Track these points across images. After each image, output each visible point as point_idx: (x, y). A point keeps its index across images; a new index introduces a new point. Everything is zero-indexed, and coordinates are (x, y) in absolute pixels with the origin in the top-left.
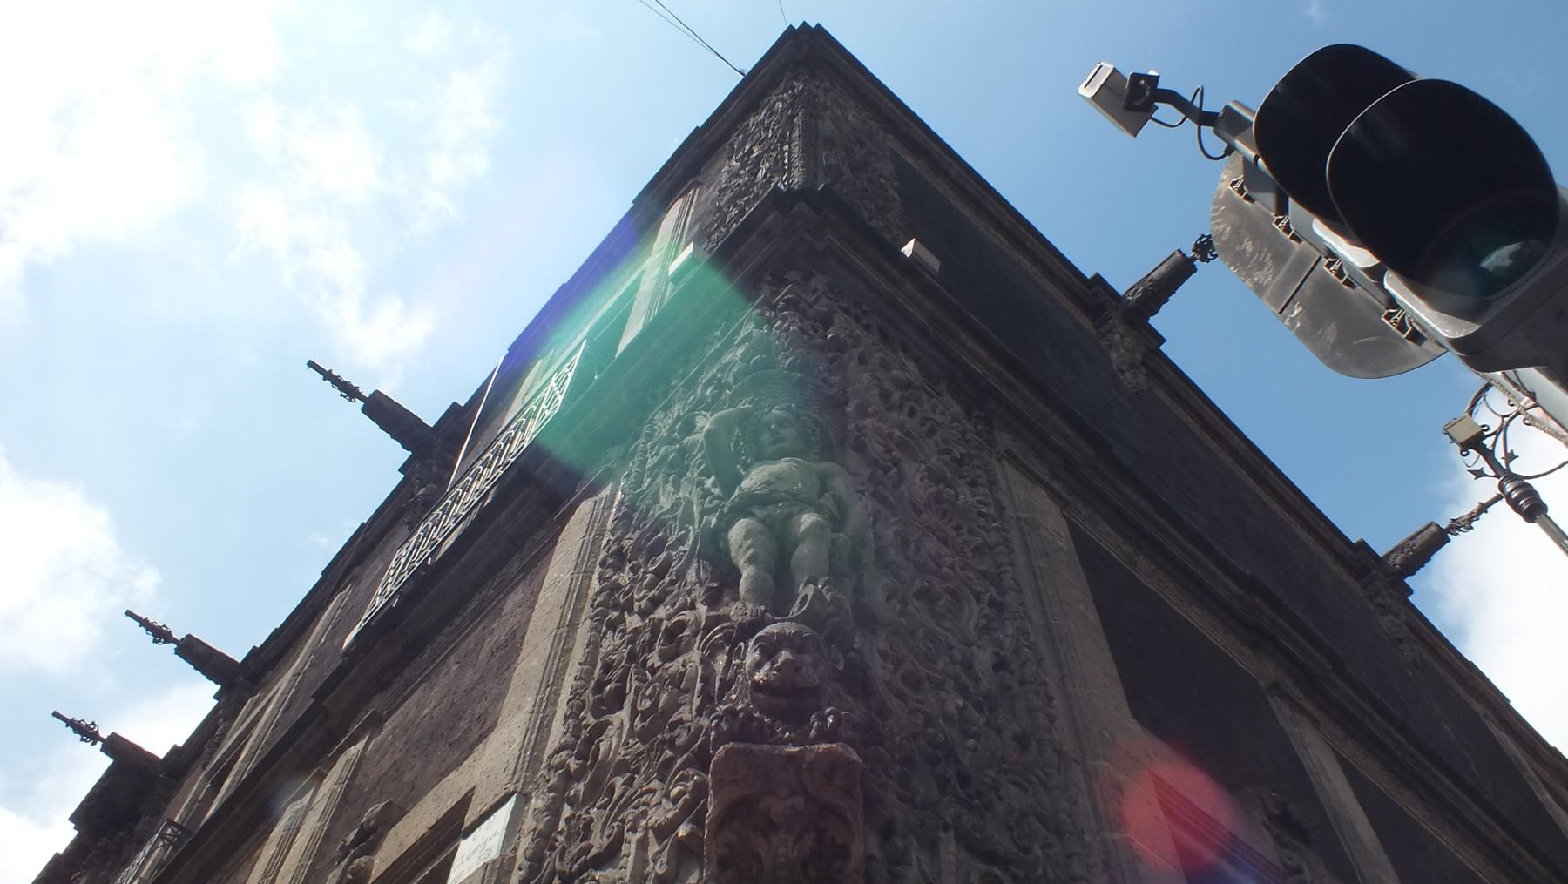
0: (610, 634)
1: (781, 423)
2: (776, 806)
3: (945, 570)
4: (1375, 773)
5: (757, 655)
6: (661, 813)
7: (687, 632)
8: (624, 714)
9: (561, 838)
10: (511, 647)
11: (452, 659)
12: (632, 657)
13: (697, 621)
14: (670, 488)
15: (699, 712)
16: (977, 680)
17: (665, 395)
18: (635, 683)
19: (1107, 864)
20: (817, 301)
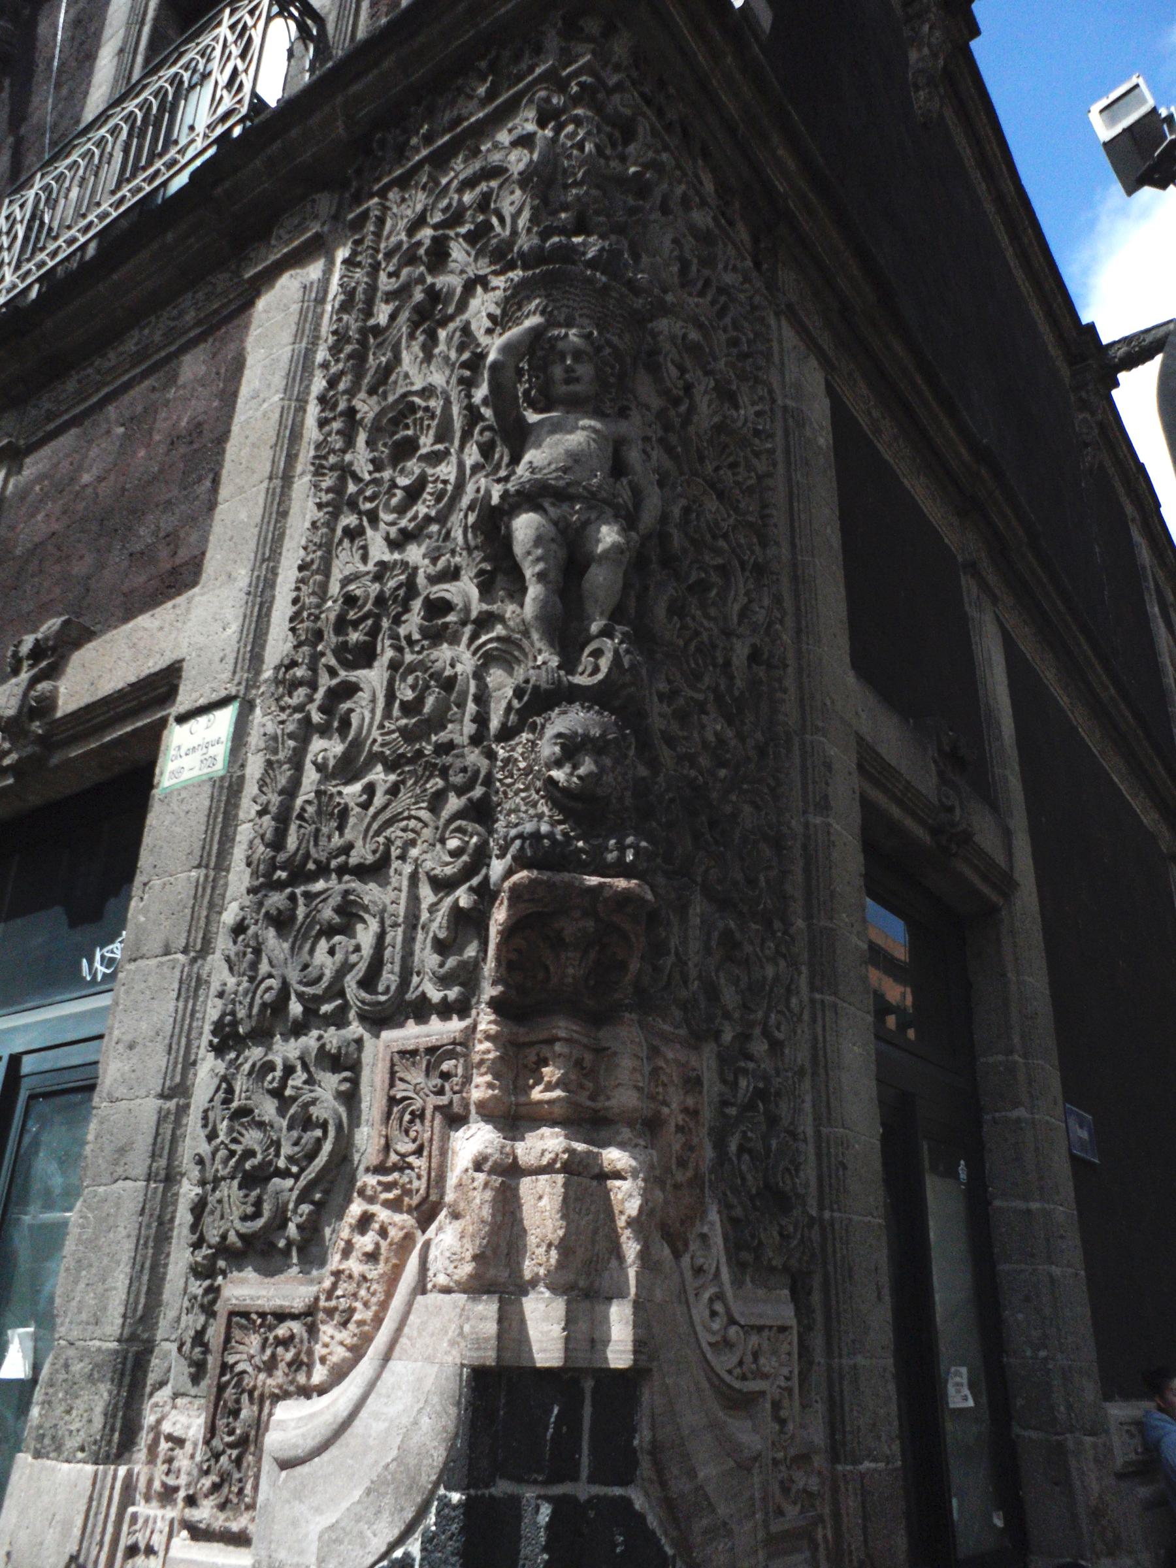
0: (346, 543)
1: (578, 355)
2: (570, 927)
3: (721, 543)
5: (557, 749)
6: (439, 862)
7: (451, 618)
8: (373, 678)
9: (311, 809)
11: (111, 410)
12: (380, 600)
13: (467, 609)
14: (416, 347)
15: (476, 740)
16: (732, 678)
18: (389, 653)
19: (805, 847)
20: (619, 87)
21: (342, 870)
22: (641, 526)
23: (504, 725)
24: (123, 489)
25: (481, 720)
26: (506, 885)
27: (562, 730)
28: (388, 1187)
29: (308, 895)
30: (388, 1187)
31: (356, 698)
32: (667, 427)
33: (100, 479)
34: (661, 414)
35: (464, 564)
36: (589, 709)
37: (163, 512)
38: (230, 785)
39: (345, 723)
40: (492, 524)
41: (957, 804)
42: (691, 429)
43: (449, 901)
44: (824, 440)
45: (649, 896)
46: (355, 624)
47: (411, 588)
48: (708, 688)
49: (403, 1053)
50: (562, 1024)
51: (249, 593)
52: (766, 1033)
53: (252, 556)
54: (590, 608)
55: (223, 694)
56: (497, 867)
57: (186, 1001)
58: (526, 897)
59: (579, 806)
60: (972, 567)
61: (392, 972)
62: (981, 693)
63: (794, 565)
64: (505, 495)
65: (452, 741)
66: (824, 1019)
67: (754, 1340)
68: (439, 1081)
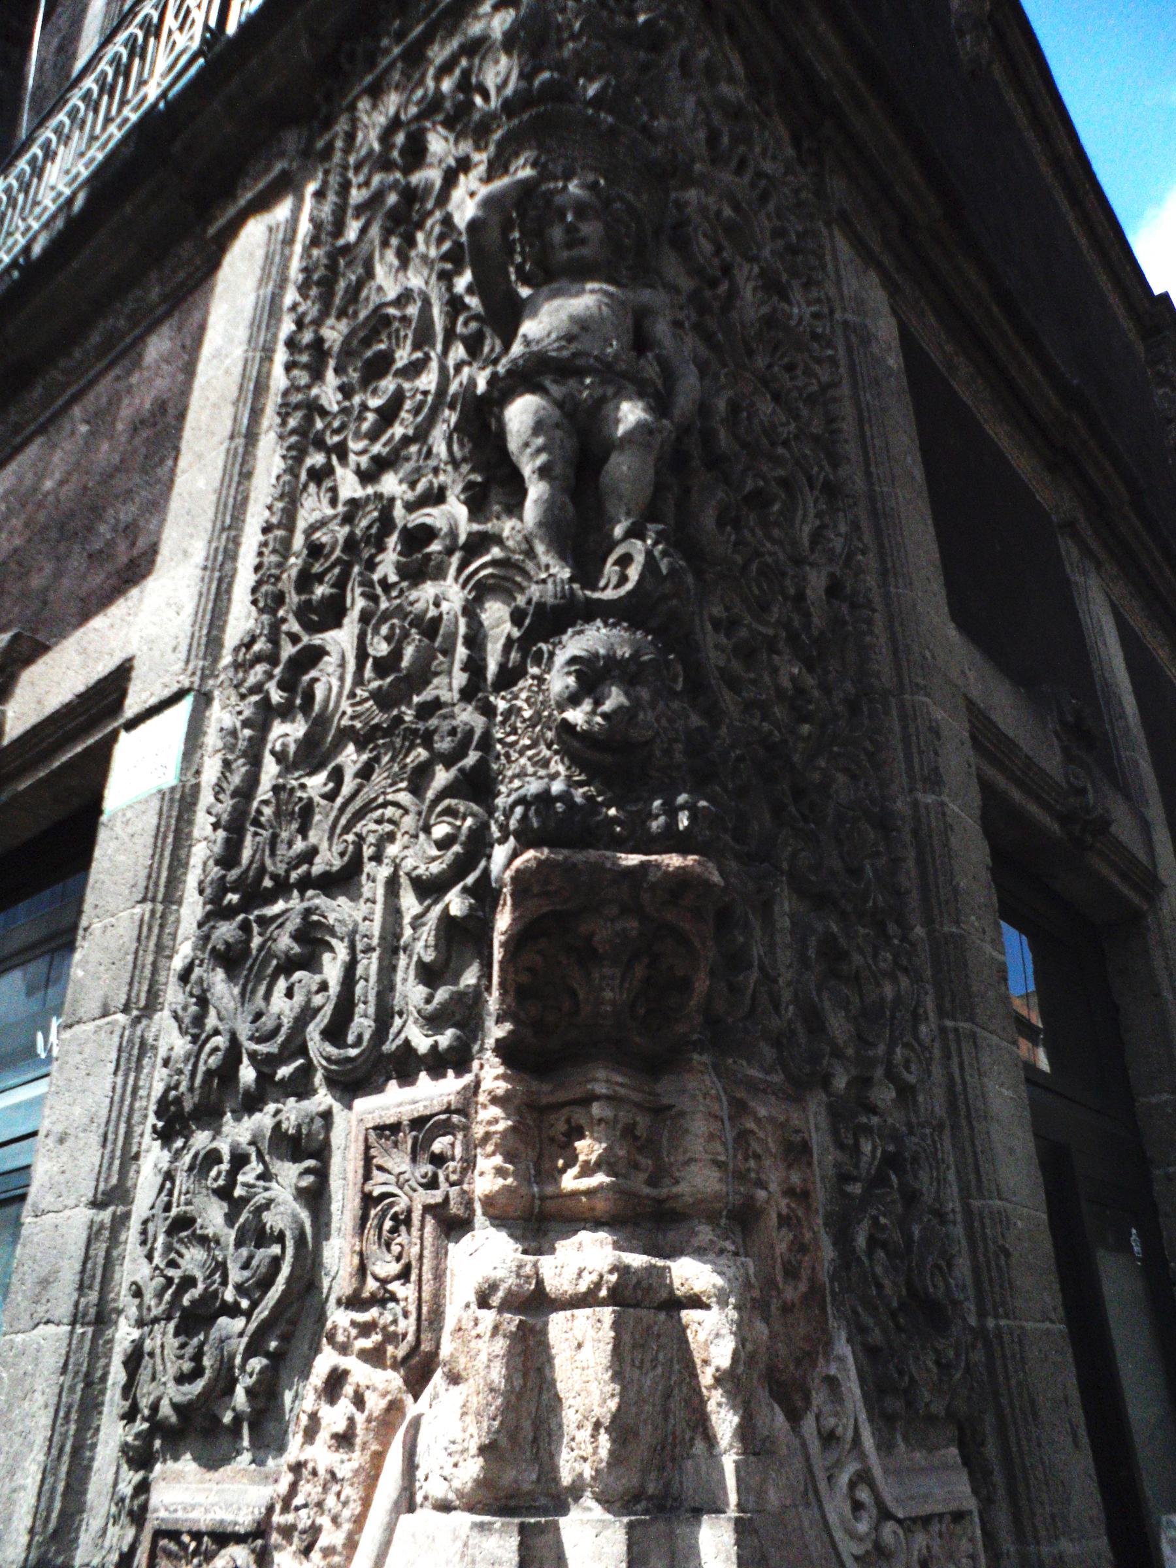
0: (312, 488)
1: (581, 209)
2: (603, 931)
3: (780, 450)
4: (1138, 622)
5: (571, 680)
6: (420, 856)
7: (435, 547)
9: (268, 811)
10: (163, 428)
11: (77, 411)
12: (351, 544)
13: (453, 533)
14: (391, 256)
15: (467, 694)
16: (807, 615)
17: (372, 64)
18: (361, 603)
19: (915, 833)
21: (305, 884)
22: (677, 412)
23: (502, 667)
24: (85, 488)
25: (475, 666)
26: (508, 874)
27: (578, 653)
28: (366, 1329)
29: (264, 922)
30: (366, 1329)
31: (321, 665)
32: (703, 309)
33: (62, 483)
34: (694, 296)
35: (449, 481)
36: (614, 625)
37: (124, 503)
38: (183, 797)
39: (309, 696)
40: (480, 420)
41: (1089, 786)
42: (734, 315)
43: (437, 910)
44: (894, 361)
45: (716, 878)
46: (320, 578)
47: (386, 522)
48: (778, 621)
49: (380, 1129)
50: (601, 1074)
51: (205, 568)
52: (891, 1076)
53: (209, 526)
54: (611, 507)
55: (175, 688)
56: (500, 853)
57: (126, 1076)
58: (536, 890)
59: (608, 759)
60: (1070, 526)
61: (365, 1016)
62: (1095, 665)
63: (872, 498)
64: (493, 380)
65: (437, 698)
66: (960, 1055)
67: (920, 1539)
68: (429, 1168)
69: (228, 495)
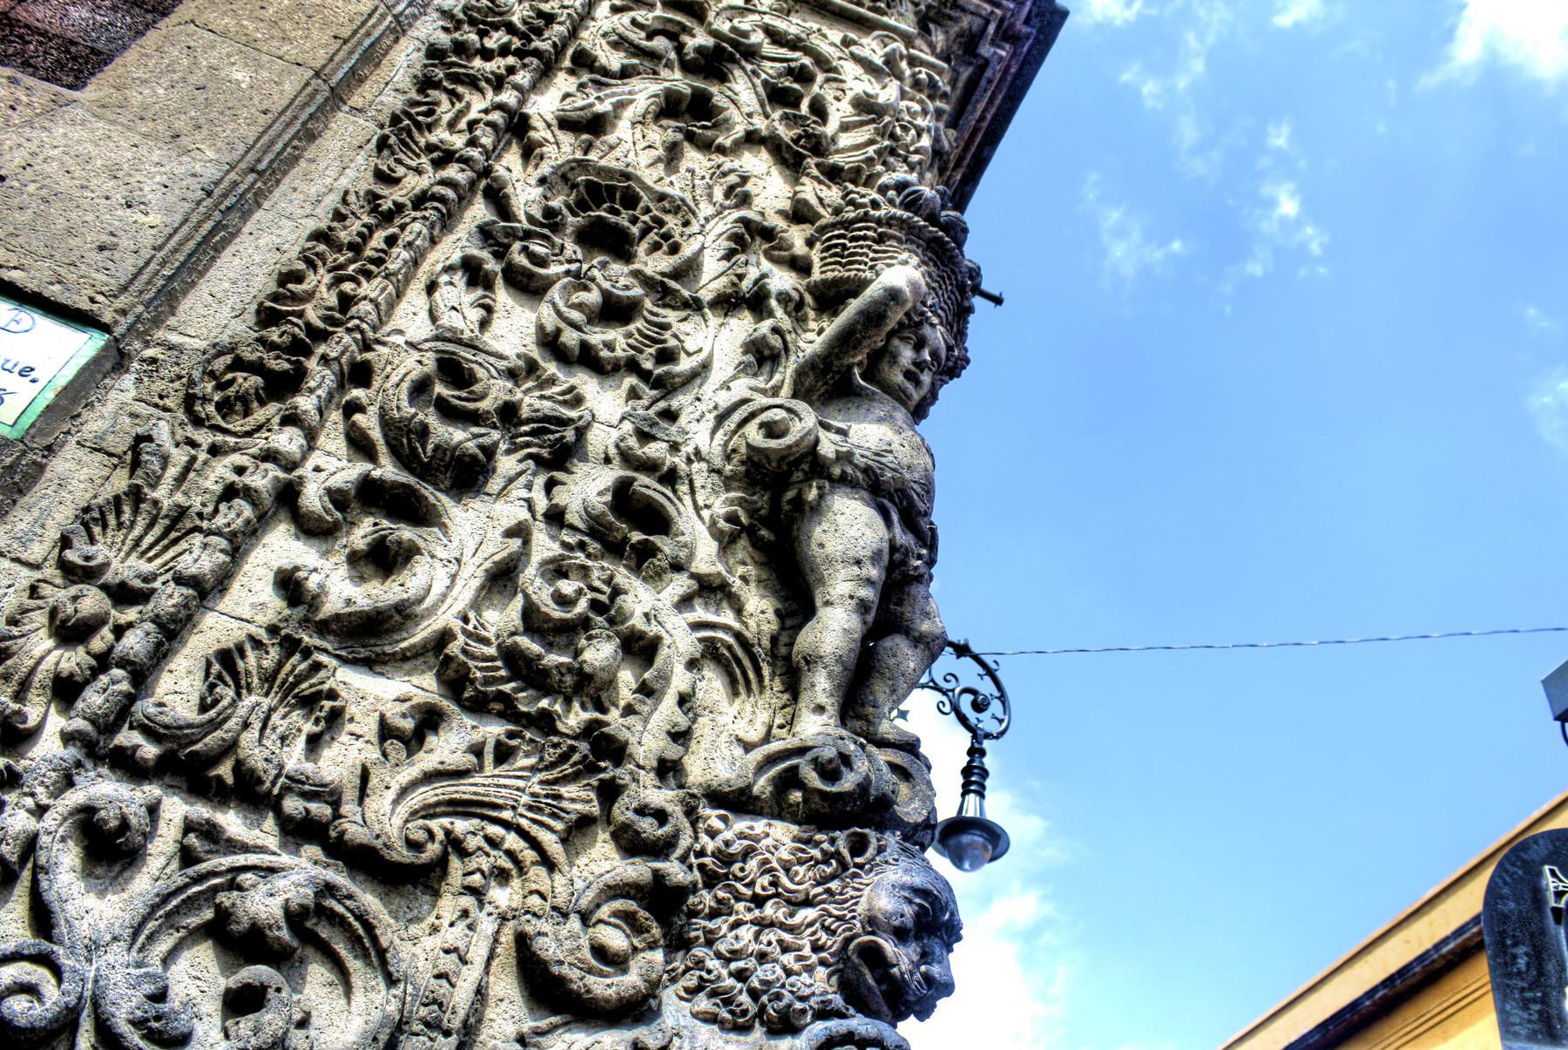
5: (909, 910)
69: (280, 135)
